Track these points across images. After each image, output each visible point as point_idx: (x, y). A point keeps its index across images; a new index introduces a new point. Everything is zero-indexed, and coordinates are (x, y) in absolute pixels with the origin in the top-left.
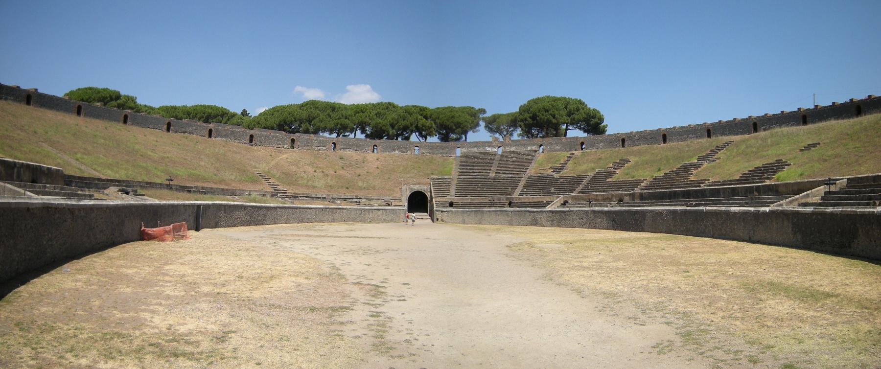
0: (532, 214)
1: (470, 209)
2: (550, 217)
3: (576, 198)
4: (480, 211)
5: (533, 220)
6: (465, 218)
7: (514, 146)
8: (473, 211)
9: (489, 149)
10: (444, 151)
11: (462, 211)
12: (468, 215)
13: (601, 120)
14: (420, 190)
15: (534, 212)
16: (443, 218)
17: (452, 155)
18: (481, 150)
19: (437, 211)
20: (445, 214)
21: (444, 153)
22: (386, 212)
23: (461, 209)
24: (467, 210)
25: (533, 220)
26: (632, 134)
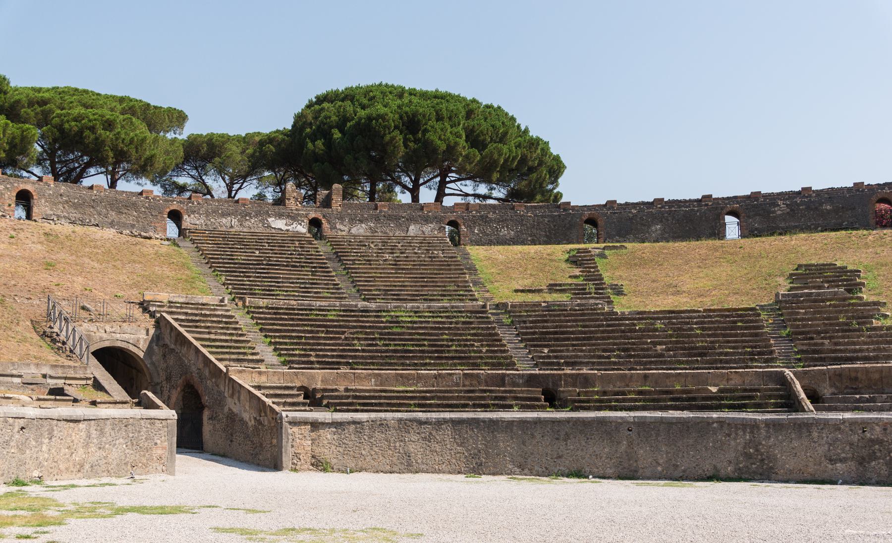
0: (744, 437)
1: (434, 415)
2: (851, 444)
3: (856, 379)
4: (477, 421)
5: (748, 456)
6: (412, 448)
7: (361, 221)
8: (445, 421)
9: (279, 224)
10: (123, 219)
11: (400, 420)
12: (424, 439)
13: (556, 169)
14: (119, 344)
15: (753, 426)
16: (317, 451)
17: (151, 234)
18: (253, 224)
19: (294, 423)
20: (327, 435)
21: (125, 226)
22: (102, 432)
23: (399, 415)
24: (421, 415)
25: (748, 456)
26: (757, 200)
